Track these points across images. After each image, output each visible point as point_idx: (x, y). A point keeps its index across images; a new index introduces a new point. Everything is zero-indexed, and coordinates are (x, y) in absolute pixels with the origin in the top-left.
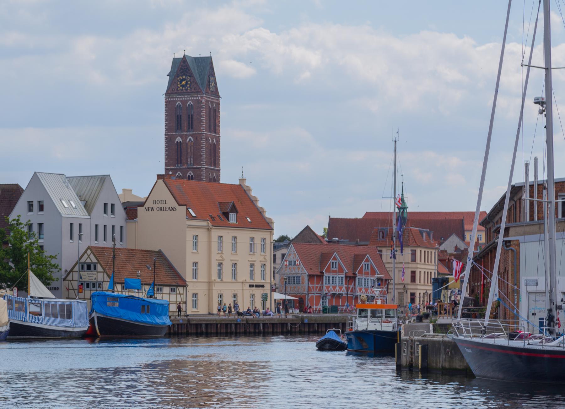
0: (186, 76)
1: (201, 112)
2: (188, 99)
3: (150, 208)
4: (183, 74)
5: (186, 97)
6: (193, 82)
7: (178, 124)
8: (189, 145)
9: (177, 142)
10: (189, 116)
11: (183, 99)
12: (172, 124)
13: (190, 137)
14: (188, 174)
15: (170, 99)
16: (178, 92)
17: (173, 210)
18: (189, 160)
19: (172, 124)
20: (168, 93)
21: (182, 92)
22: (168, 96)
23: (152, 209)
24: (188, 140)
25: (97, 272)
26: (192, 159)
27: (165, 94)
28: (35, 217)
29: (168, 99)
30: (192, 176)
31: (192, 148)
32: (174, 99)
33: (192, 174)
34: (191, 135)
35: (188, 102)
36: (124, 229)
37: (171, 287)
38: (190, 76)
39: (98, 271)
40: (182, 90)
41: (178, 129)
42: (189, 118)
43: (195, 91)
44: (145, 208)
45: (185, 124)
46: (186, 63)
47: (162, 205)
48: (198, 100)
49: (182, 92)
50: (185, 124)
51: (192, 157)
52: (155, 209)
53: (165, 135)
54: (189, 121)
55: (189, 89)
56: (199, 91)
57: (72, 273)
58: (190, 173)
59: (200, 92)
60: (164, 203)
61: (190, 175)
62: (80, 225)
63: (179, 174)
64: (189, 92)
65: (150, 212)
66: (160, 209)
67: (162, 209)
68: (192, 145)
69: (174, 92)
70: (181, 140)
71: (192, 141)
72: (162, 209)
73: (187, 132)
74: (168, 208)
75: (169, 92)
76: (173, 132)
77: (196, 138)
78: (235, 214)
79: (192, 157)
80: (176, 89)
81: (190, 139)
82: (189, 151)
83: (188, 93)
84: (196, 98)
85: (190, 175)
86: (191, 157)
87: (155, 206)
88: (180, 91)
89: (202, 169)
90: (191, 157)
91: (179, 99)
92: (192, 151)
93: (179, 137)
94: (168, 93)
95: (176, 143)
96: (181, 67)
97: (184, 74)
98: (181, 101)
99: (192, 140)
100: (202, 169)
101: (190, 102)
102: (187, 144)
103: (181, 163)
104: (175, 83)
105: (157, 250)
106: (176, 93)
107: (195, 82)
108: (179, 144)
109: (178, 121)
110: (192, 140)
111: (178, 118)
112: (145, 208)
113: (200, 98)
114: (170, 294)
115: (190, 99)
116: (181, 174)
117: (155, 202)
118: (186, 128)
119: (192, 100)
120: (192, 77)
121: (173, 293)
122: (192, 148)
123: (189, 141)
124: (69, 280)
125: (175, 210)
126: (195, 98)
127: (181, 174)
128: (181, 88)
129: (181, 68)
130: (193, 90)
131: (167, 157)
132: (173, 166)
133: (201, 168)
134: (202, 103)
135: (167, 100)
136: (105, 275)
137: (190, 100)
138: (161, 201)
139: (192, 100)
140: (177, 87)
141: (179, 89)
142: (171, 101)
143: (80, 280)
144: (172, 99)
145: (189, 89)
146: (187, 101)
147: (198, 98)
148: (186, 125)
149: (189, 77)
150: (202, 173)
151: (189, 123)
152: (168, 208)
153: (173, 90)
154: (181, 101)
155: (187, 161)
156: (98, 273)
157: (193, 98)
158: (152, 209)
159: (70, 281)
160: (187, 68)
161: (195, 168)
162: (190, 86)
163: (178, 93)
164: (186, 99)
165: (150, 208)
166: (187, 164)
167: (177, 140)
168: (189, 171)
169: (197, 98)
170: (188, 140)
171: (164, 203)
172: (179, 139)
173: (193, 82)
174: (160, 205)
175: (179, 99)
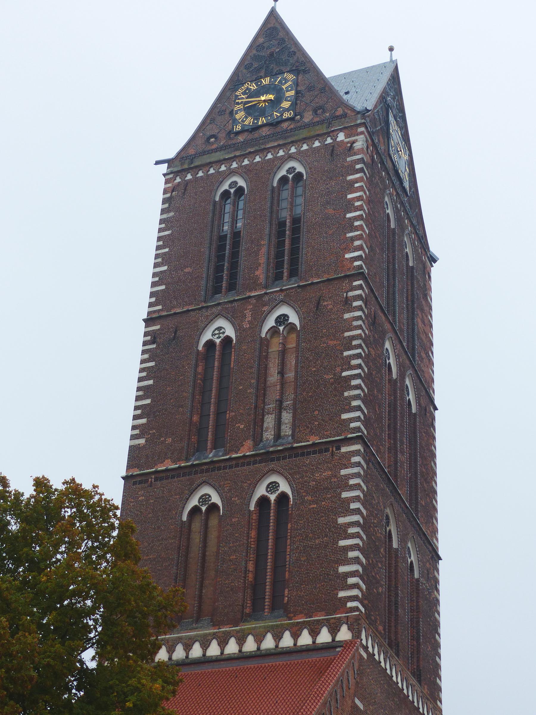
8: (275, 347)
9: (210, 344)
10: (282, 224)
14: (261, 491)
15: (189, 177)
16: (230, 142)
18: (269, 421)
24: (270, 323)
26: (287, 417)
27: (169, 162)
30: (283, 496)
31: (291, 361)
33: (284, 487)
41: (217, 290)
42: (281, 234)
53: (148, 322)
54: (280, 244)
56: (340, 112)
58: (273, 487)
61: (273, 497)
63: (205, 498)
68: (292, 345)
69: (214, 146)
70: (230, 331)
71: (292, 327)
79: (288, 403)
81: (282, 319)
82: (273, 377)
85: (273, 497)
89: (344, 450)
90: (280, 408)
92: (290, 375)
95: (200, 348)
99: (294, 319)
100: (344, 450)
102: (265, 343)
110: (294, 319)
113: (341, 137)
116: (216, 499)
122: (291, 361)
123: (274, 331)
127: (216, 499)
132: (174, 462)
134: (355, 154)
135: (178, 180)
148: (262, 260)
150: (343, 472)
151: (280, 254)
161: (303, 452)
166: (258, 439)
168: (264, 476)
169: (329, 141)
170: (270, 323)
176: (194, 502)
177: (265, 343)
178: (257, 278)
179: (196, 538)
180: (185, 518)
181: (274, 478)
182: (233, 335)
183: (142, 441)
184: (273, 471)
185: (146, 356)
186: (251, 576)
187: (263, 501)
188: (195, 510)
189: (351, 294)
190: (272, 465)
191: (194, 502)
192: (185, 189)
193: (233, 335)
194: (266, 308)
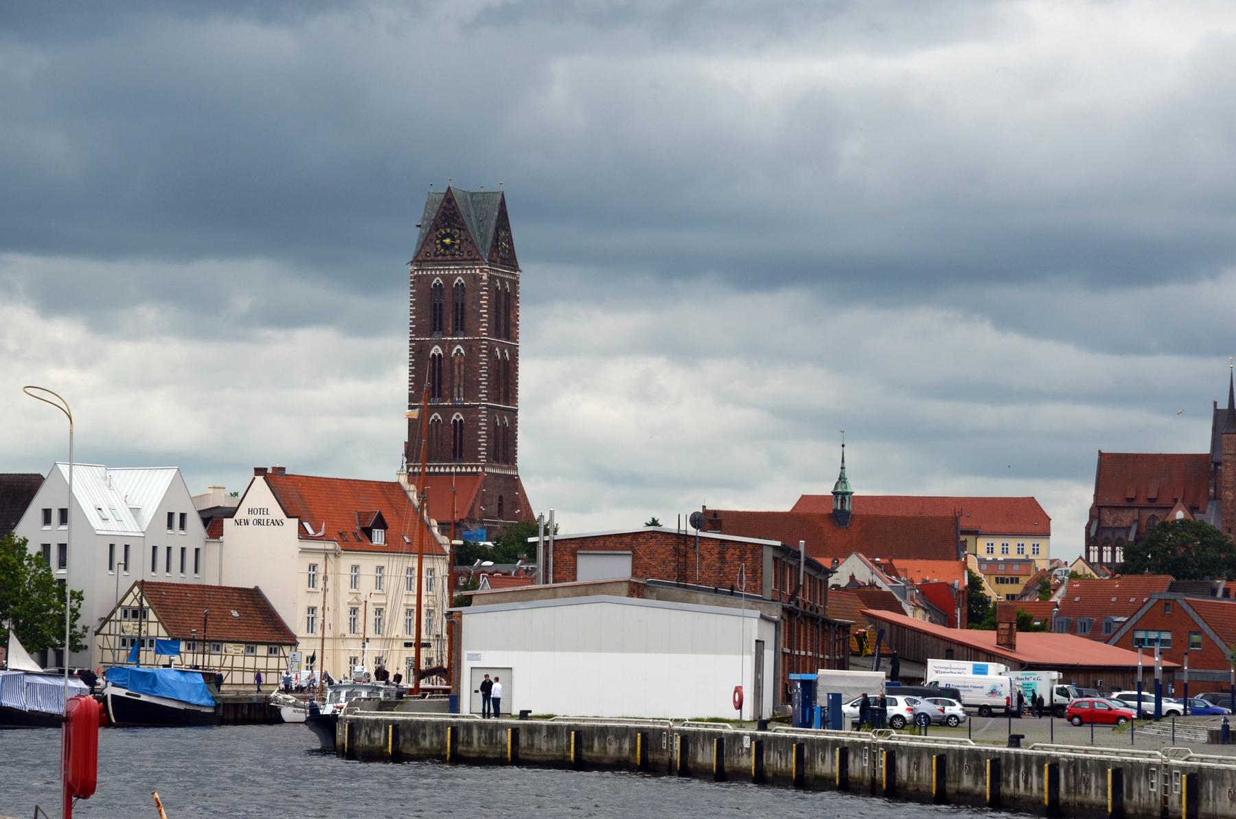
0: (452, 227)
1: (481, 298)
2: (456, 272)
3: (243, 521)
4: (446, 224)
5: (452, 269)
6: (466, 240)
7: (435, 320)
9: (434, 355)
10: (457, 304)
11: (447, 272)
12: (423, 320)
13: (459, 347)
14: (454, 417)
15: (420, 273)
16: (436, 258)
17: (278, 524)
18: (456, 390)
19: (423, 320)
20: (418, 261)
21: (445, 258)
22: (417, 265)
23: (247, 523)
24: (454, 352)
25: (148, 622)
26: (461, 389)
28: (55, 534)
29: (418, 272)
30: (461, 420)
31: (462, 368)
32: (429, 273)
33: (461, 417)
34: (460, 343)
35: (455, 279)
36: (201, 553)
37: (270, 646)
38: (460, 229)
39: (149, 620)
40: (444, 255)
41: (435, 330)
42: (457, 309)
43: (468, 258)
44: (236, 520)
45: (449, 321)
46: (453, 204)
47: (262, 517)
48: (475, 276)
49: (445, 258)
50: (449, 321)
51: (462, 384)
52: (251, 523)
54: (457, 314)
55: (457, 253)
56: (477, 257)
57: (108, 623)
58: (458, 416)
59: (478, 260)
60: (265, 513)
61: (458, 420)
62: (127, 547)
63: (436, 417)
64: (456, 260)
65: (243, 527)
66: (259, 522)
67: (262, 523)
68: (462, 361)
69: (429, 259)
70: (441, 352)
72: (262, 523)
73: (452, 336)
74: (270, 521)
75: (420, 259)
76: (426, 337)
77: (471, 349)
78: (383, 530)
79: (462, 384)
80: (432, 253)
81: (458, 350)
83: (454, 262)
84: (471, 271)
85: (458, 420)
86: (459, 385)
87: (251, 518)
88: (440, 258)
89: (480, 408)
90: (459, 385)
91: (438, 273)
92: (462, 373)
93: (437, 347)
94: (418, 261)
95: (431, 356)
96: (442, 210)
97: (449, 226)
98: (442, 277)
99: (463, 352)
100: (480, 408)
101: (459, 278)
102: (453, 359)
103: (440, 396)
104: (431, 240)
105: (252, 586)
106: (432, 261)
107: (470, 240)
108: (437, 359)
109: (435, 315)
110: (463, 352)
111: (435, 310)
112: (236, 520)
113: (478, 271)
114: (267, 657)
115: (460, 272)
116: (439, 418)
117: (251, 511)
118: (450, 329)
119: (462, 275)
120: (464, 230)
121: (273, 655)
122: (462, 368)
123: (456, 354)
124: (104, 635)
125: (281, 524)
126: (469, 272)
127: (439, 418)
128: (442, 250)
129: (443, 214)
130: (465, 256)
131: (412, 384)
133: (478, 406)
135: (416, 273)
136: (160, 624)
137: (459, 275)
138: (260, 509)
139: (462, 275)
140: (435, 250)
141: (438, 253)
142: (423, 275)
143: (122, 634)
144: (425, 273)
145: (457, 253)
146: (454, 276)
147: (475, 271)
148: (451, 324)
149: (457, 231)
150: (480, 416)
151: (457, 319)
152: (270, 521)
153: (426, 255)
154: (442, 277)
155: (452, 391)
156: (149, 624)
157: (464, 272)
158: (247, 523)
159: (106, 635)
160: (455, 214)
161: (467, 406)
162: (460, 248)
163: (437, 261)
164: (451, 272)
165: (243, 521)
166: (452, 397)
167: (432, 352)
169: (473, 272)
170: (454, 352)
171: (265, 513)
172: (436, 350)
173: (466, 240)
174: (258, 517)
175: (438, 273)
176: (433, 418)
177: (453, 359)
178: (449, 331)
179: (434, 430)
180: (430, 423)
181: (458, 413)
182: (442, 353)
183: (413, 392)
184: (458, 411)
185: (411, 356)
186: (452, 447)
187: (455, 421)
188: (433, 420)
189: (482, 347)
190: (458, 409)
191: (433, 418)
192: (419, 279)
193: (442, 353)
194: (453, 346)
